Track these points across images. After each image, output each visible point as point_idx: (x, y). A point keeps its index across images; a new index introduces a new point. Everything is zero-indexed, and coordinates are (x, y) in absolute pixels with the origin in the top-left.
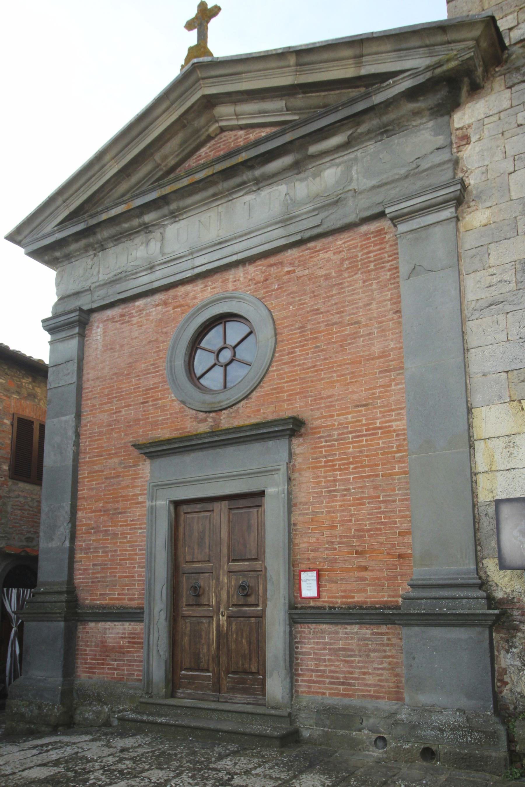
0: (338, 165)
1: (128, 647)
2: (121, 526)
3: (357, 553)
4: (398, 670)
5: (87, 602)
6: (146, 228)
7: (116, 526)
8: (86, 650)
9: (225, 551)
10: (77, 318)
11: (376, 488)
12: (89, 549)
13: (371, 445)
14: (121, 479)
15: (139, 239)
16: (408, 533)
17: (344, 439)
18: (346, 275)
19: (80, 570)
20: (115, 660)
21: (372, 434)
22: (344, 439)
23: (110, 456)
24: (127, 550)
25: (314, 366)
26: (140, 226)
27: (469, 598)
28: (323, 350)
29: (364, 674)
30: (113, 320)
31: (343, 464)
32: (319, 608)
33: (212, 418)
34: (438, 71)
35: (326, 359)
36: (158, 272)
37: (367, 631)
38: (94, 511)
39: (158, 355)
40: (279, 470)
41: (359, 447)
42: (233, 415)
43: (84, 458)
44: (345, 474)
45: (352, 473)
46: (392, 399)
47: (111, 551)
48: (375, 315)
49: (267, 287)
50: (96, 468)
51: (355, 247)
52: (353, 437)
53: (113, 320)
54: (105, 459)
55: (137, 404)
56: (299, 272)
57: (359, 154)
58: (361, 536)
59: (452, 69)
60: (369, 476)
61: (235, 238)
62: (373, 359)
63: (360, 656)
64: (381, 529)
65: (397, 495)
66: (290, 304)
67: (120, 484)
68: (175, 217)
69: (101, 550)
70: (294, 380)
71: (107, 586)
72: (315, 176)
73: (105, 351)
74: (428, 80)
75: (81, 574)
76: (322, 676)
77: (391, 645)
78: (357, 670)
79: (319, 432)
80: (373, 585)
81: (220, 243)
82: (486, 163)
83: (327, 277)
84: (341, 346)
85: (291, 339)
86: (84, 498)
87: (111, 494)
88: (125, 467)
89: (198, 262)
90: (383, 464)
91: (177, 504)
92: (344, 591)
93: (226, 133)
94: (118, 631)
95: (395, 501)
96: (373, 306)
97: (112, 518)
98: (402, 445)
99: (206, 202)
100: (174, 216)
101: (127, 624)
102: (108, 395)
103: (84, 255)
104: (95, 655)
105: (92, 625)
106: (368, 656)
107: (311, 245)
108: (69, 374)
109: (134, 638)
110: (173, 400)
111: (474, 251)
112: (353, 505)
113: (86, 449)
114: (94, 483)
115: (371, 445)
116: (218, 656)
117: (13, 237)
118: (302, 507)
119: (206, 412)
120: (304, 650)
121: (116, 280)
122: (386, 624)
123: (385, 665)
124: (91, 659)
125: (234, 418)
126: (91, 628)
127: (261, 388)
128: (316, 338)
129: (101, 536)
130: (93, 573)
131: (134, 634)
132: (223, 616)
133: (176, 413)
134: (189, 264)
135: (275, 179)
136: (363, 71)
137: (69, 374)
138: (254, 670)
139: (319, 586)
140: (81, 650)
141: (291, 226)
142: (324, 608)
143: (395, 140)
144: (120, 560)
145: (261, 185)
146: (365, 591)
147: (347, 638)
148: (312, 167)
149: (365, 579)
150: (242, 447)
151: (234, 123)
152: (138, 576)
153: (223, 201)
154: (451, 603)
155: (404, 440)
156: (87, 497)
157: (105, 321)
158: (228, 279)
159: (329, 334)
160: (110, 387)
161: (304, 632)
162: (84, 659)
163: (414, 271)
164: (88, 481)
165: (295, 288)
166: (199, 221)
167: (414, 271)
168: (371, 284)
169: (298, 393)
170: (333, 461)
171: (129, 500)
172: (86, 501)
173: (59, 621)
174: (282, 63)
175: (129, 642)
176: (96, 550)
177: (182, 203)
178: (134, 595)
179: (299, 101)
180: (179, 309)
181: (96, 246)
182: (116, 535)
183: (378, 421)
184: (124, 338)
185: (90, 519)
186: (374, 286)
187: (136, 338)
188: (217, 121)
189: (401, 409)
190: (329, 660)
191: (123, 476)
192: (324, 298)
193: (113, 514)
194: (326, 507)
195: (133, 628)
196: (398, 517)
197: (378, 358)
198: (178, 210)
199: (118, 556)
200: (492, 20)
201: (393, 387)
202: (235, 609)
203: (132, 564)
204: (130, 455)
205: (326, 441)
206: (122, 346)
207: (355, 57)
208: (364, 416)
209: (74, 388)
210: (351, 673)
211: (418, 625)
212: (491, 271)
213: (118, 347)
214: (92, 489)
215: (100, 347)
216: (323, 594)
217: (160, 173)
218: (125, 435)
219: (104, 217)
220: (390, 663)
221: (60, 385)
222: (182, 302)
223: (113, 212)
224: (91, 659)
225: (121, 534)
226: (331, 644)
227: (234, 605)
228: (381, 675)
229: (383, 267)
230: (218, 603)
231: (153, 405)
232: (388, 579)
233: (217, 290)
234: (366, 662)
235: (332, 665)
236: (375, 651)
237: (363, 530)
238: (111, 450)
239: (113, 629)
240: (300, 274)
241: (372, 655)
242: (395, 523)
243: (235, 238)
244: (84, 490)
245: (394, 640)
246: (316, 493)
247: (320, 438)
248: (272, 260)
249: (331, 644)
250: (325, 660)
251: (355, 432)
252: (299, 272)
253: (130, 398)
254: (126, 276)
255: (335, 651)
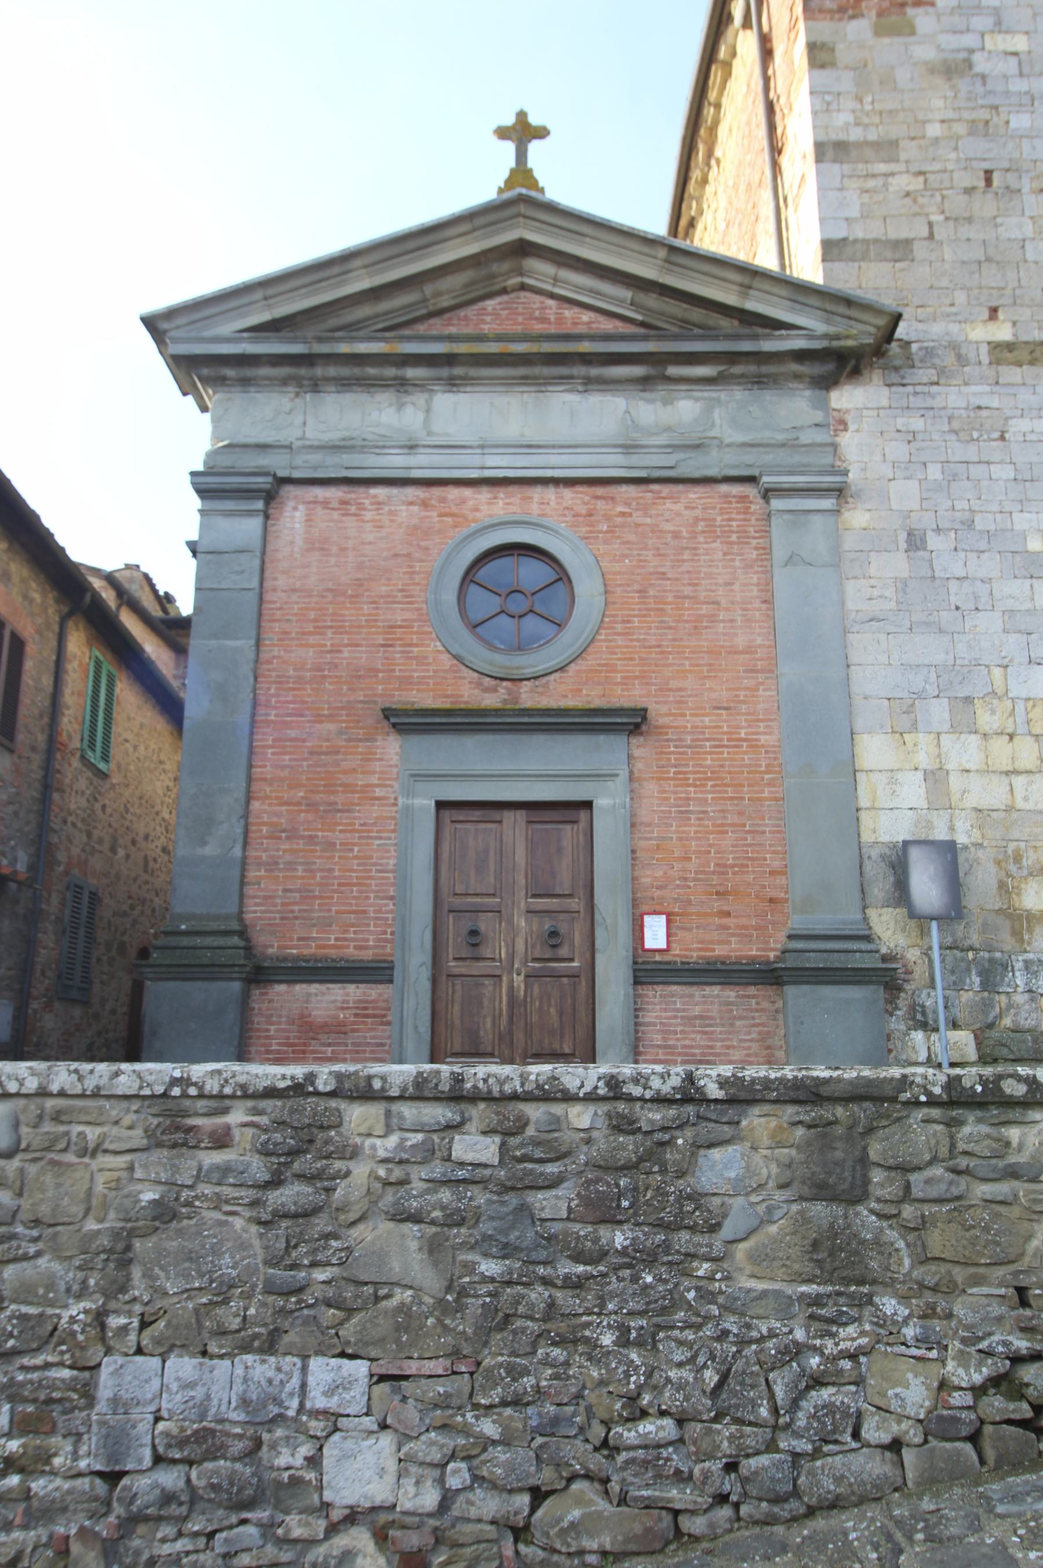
0: (697, 400)
1: (354, 1023)
2: (341, 831)
3: (717, 893)
4: (769, 1042)
5: (270, 951)
6: (402, 385)
7: (333, 831)
8: (268, 1030)
9: (522, 881)
10: (268, 486)
11: (741, 813)
12: (277, 863)
13: (734, 760)
14: (341, 757)
15: (384, 397)
16: (783, 873)
17: (701, 747)
18: (702, 539)
19: (255, 897)
20: (329, 1045)
21: (736, 746)
22: (701, 747)
23: (319, 719)
24: (352, 871)
25: (659, 646)
26: (395, 379)
27: (861, 951)
28: (670, 628)
29: (728, 1047)
30: (325, 504)
31: (699, 779)
32: (668, 963)
33: (506, 688)
34: (835, 344)
35: (675, 640)
36: (421, 457)
37: (730, 994)
38: (286, 804)
39: (411, 579)
40: (617, 775)
41: (719, 760)
42: (540, 689)
43: (266, 715)
44: (701, 792)
45: (709, 792)
46: (761, 706)
47: (322, 870)
48: (738, 599)
49: (592, 525)
50: (292, 733)
51: (714, 508)
52: (711, 747)
53: (325, 504)
54: (309, 722)
55: (373, 645)
56: (637, 517)
57: (723, 396)
58: (723, 873)
59: (850, 348)
60: (731, 799)
61: (553, 447)
62: (736, 653)
63: (723, 1025)
64: (747, 866)
65: (767, 825)
66: (626, 556)
67: (338, 765)
68: (454, 385)
69: (300, 868)
70: (632, 659)
71: (314, 925)
72: (666, 402)
73: (308, 550)
74: (824, 349)
75: (257, 905)
76: (673, 1054)
77: (762, 1010)
78: (719, 1044)
79: (667, 734)
80: (737, 935)
81: (530, 446)
82: (865, 459)
83: (676, 535)
84: (696, 627)
85: (626, 603)
86: (265, 780)
87: (321, 779)
88: (349, 740)
89: (491, 461)
90: (749, 785)
91: (441, 805)
92: (702, 942)
93: (528, 294)
94: (333, 998)
95: (764, 832)
96: (736, 587)
97: (322, 818)
98: (773, 766)
99: (509, 383)
100: (453, 384)
101: (351, 988)
102: (315, 620)
103: (277, 388)
104: (288, 1038)
105: (282, 988)
106: (732, 1025)
107: (655, 487)
108: (243, 572)
109: (366, 1008)
110: (438, 651)
111: (854, 555)
112: (712, 833)
113: (269, 701)
114: (287, 757)
115: (734, 760)
116: (510, 1032)
117: (151, 323)
118: (643, 829)
119: (496, 678)
120: (646, 1020)
121: (344, 447)
122: (755, 984)
123: (754, 1036)
124: (279, 1044)
125: (542, 694)
126: (278, 994)
127: (583, 659)
128: (662, 609)
129: (301, 844)
130: (283, 904)
131: (367, 1002)
132: (518, 974)
133: (446, 671)
134: (476, 460)
135: (611, 387)
136: (750, 305)
137: (243, 572)
138: (567, 1051)
139: (669, 935)
140: (258, 1030)
141: (635, 456)
142: (675, 963)
143: (768, 396)
144: (339, 885)
145: (590, 387)
146: (729, 943)
147: (705, 1003)
148: (662, 391)
149: (728, 928)
150: (560, 738)
151: (548, 287)
152: (375, 912)
153: (532, 389)
154: (842, 956)
155: (775, 759)
156: (273, 779)
157: (309, 503)
158: (531, 498)
159: (679, 609)
160: (320, 609)
161: (647, 996)
162: (264, 1045)
163: (790, 561)
164: (273, 754)
165: (632, 538)
166: (492, 403)
167: (790, 561)
168: (733, 560)
169: (636, 677)
170: (685, 773)
171: (357, 792)
172: (270, 785)
173: (232, 979)
174: (646, 250)
175: (356, 1015)
176: (291, 866)
177: (473, 372)
178: (368, 940)
179: (652, 301)
180: (449, 520)
181: (305, 382)
182: (330, 845)
183: (743, 731)
184: (348, 538)
185: (278, 815)
186: (737, 563)
187: (370, 543)
188: (521, 275)
189: (771, 720)
190: (682, 1032)
191: (345, 753)
192: (673, 561)
193: (325, 811)
194: (677, 832)
195: (364, 994)
196: (769, 852)
197: (742, 652)
198: (461, 378)
199: (335, 878)
200: (898, 318)
201: (761, 692)
202: (537, 965)
203: (361, 892)
204: (358, 722)
205: (676, 747)
206: (343, 549)
207: (741, 285)
208: (725, 721)
209: (252, 597)
210: (711, 1047)
211: (808, 983)
212: (872, 582)
213: (334, 549)
214: (283, 768)
215: (299, 541)
216: (674, 945)
217: (424, 311)
218: (349, 689)
219: (344, 348)
220: (759, 1033)
221: (223, 586)
222: (454, 509)
223: (362, 348)
224: (279, 1044)
225: (341, 844)
226: (684, 1010)
227: (535, 960)
228: (749, 1048)
229: (747, 543)
230: (512, 956)
231: (402, 652)
232: (757, 928)
233: (514, 509)
234: (730, 1033)
235: (685, 1039)
236: (740, 1018)
237: (725, 866)
238: (323, 709)
239: (323, 994)
240: (640, 520)
241: (738, 1023)
242: (765, 859)
243: (553, 447)
244: (265, 766)
245: (765, 1005)
246: (663, 812)
247: (668, 740)
248: (600, 491)
249: (684, 1010)
250: (676, 1033)
251: (714, 740)
252: (637, 517)
253: (359, 633)
254: (363, 447)
255: (690, 1020)
